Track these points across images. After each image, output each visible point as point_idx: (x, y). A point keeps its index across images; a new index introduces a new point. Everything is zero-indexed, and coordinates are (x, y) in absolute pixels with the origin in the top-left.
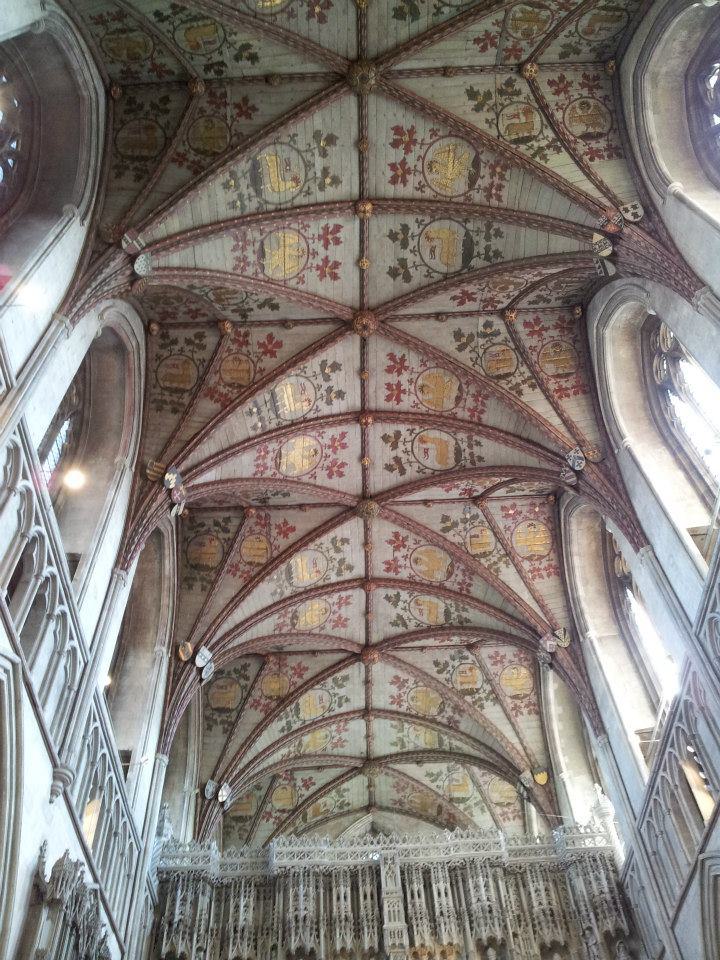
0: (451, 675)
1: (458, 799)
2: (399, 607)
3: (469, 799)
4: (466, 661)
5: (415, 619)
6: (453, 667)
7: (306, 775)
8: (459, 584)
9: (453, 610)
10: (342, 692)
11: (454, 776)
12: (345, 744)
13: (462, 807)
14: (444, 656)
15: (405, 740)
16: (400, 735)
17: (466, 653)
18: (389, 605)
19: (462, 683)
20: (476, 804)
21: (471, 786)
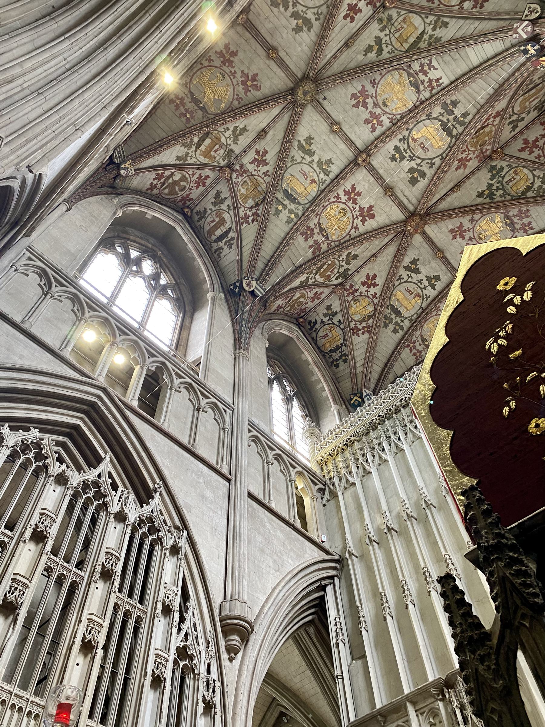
0: (339, 261)
1: (204, 140)
2: (425, 279)
3: (196, 151)
4: (336, 277)
5: (406, 281)
6: (342, 266)
7: (360, 19)
8: (414, 342)
9: (398, 319)
10: (406, 165)
11: (222, 151)
12: (354, 102)
13: (196, 140)
14: (354, 265)
15: (308, 159)
16: (316, 158)
17: (340, 280)
18: (432, 275)
19: (329, 265)
20: (187, 154)
21: (203, 160)
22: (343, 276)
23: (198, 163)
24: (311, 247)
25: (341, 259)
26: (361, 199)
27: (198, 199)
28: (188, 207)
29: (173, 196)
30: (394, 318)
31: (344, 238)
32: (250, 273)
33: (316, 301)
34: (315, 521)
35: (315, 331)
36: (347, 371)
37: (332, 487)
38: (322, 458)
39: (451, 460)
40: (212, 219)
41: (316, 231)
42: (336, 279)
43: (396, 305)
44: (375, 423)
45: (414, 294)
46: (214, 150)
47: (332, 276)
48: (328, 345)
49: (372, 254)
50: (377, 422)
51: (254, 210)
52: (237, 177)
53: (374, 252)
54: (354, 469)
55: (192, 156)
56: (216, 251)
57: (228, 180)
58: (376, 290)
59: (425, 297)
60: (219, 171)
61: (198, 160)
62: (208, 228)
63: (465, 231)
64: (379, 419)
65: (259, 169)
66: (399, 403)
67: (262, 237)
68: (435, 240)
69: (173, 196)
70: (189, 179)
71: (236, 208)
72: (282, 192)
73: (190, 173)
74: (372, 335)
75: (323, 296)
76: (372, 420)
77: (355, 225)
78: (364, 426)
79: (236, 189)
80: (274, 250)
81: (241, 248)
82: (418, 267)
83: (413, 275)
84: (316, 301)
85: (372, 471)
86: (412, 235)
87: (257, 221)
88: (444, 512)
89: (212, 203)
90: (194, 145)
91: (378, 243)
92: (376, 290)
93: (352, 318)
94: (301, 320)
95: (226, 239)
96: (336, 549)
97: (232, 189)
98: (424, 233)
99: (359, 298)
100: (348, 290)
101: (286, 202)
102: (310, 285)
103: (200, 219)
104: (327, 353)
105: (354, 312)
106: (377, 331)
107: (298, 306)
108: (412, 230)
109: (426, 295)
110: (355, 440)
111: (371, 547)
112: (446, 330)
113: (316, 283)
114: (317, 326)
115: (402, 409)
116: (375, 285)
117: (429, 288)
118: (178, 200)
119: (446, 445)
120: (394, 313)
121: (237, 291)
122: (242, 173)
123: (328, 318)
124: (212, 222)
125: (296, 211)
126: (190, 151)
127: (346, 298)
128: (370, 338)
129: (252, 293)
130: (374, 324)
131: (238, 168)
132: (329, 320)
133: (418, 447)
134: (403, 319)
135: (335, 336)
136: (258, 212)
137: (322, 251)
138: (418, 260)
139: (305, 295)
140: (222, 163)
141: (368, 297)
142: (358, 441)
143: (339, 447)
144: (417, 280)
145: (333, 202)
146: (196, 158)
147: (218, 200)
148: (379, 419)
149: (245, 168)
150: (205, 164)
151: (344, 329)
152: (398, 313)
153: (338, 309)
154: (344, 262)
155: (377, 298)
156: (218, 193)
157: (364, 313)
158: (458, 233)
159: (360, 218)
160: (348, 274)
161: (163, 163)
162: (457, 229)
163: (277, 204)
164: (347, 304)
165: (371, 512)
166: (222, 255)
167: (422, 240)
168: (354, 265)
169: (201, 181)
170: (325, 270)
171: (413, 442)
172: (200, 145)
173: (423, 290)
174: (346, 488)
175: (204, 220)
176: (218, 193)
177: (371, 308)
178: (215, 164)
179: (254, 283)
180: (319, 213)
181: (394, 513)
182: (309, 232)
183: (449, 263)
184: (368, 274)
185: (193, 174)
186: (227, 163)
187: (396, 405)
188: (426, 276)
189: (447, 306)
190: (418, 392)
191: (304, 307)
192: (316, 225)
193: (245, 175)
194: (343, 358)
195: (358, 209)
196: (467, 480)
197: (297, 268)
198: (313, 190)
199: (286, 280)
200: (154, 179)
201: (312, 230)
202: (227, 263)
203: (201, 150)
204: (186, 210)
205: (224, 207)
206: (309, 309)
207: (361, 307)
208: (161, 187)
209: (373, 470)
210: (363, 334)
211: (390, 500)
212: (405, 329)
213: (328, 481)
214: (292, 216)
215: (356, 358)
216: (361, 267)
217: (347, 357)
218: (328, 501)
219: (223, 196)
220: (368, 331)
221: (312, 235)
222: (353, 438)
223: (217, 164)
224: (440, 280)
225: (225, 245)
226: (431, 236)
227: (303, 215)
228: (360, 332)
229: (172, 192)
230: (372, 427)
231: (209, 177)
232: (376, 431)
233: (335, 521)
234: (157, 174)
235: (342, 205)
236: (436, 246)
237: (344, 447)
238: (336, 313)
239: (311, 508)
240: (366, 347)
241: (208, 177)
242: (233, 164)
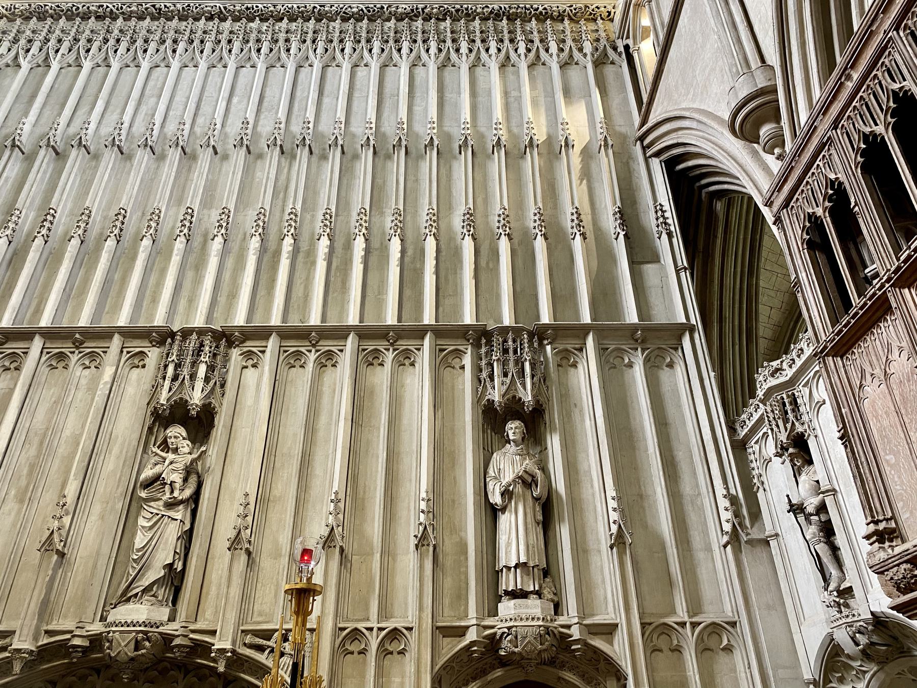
44: (47, 12)
50: (50, 11)
64: (55, 10)
66: (94, 8)
76: (45, 5)
78: (30, 5)
110: (6, 16)
115: (93, 18)
171: (70, 66)
230: (39, 13)
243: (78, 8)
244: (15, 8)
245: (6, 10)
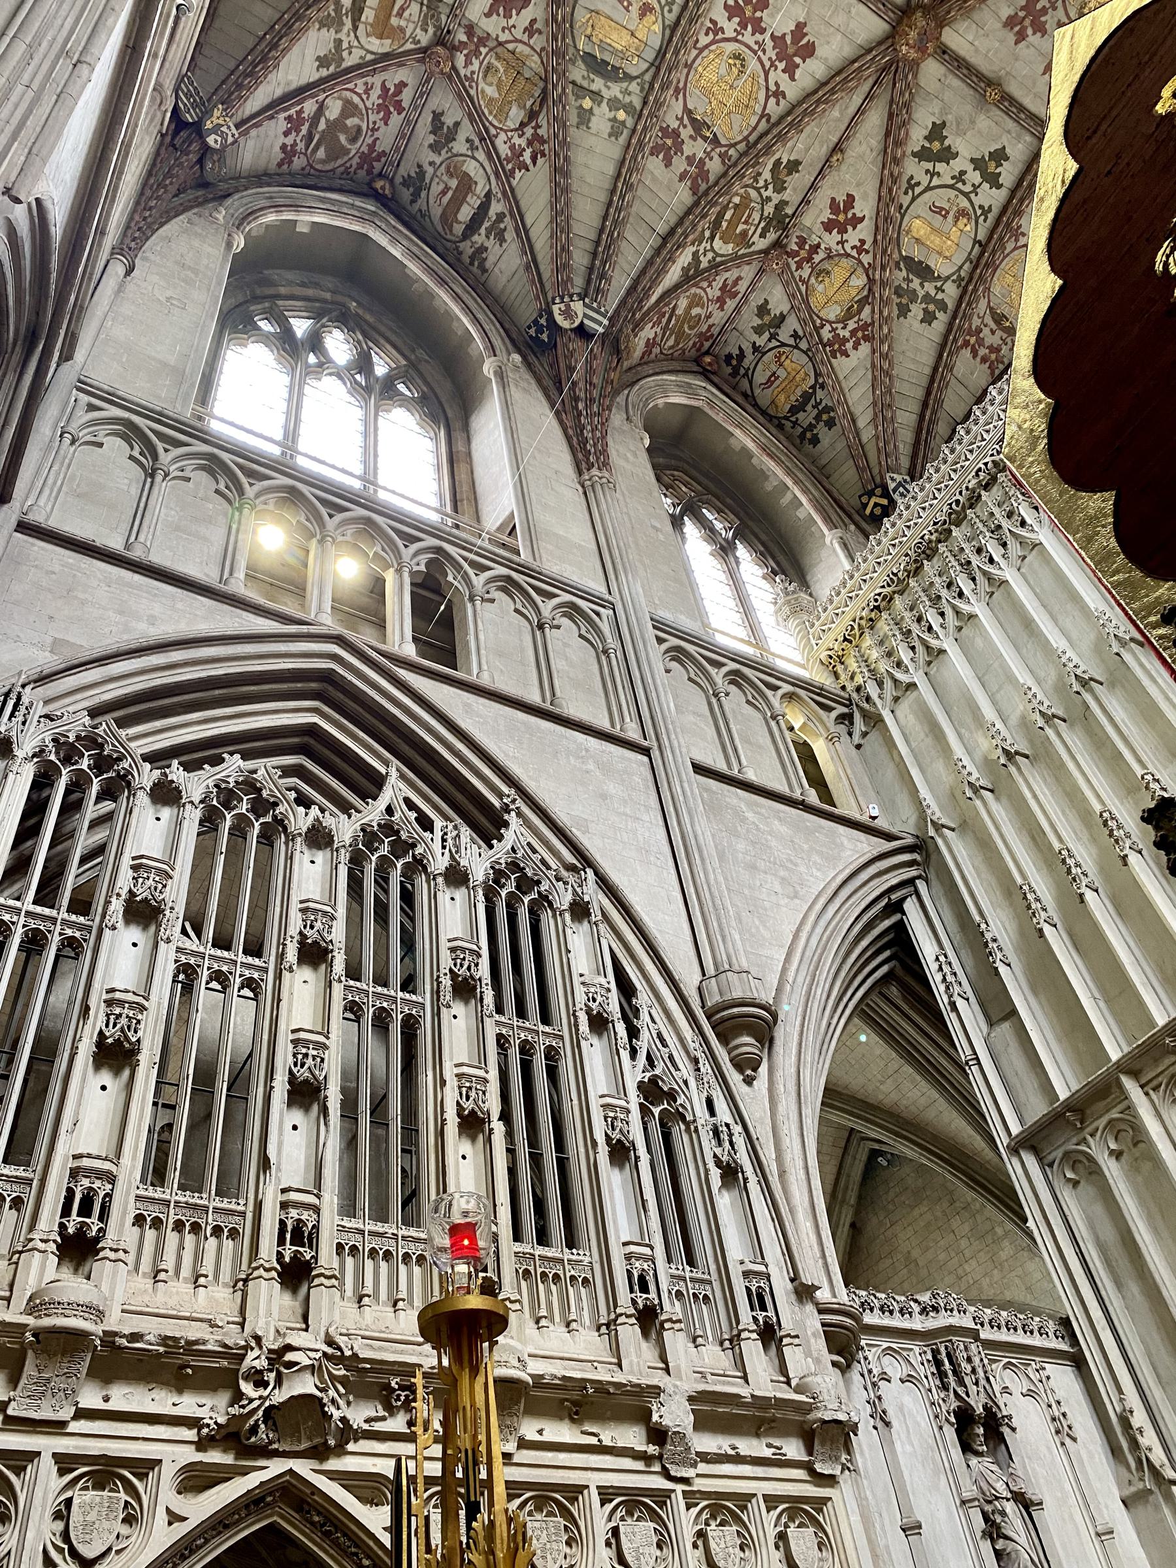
0: (757, 189)
2: (969, 167)
3: (355, 28)
4: (759, 230)
5: (928, 188)
6: (769, 199)
9: (930, 287)
17: (772, 236)
19: (736, 206)
20: (338, 42)
21: (378, 46)
22: (774, 223)
23: (369, 57)
24: (682, 177)
25: (761, 183)
26: (772, 16)
27: (398, 148)
28: (380, 175)
29: (340, 162)
30: (918, 288)
31: (755, 128)
32: (563, 286)
33: (730, 304)
34: (846, 783)
35: (746, 374)
36: (841, 445)
37: (866, 706)
38: (830, 653)
39: (1122, 556)
40: (441, 186)
41: (686, 133)
42: (762, 235)
43: (917, 254)
44: (930, 541)
45: (951, 214)
46: (395, 12)
47: (751, 233)
48: (782, 397)
49: (831, 146)
50: (933, 538)
51: (529, 131)
52: (468, 63)
53: (835, 140)
54: (905, 655)
55: (350, 47)
56: (472, 258)
57: (450, 77)
58: (863, 232)
59: (979, 212)
60: (421, 61)
61: (368, 52)
62: (439, 211)
63: (1044, 11)
64: (936, 531)
65: (511, 22)
66: (974, 482)
67: (566, 190)
68: (973, 59)
69: (340, 162)
70: (361, 106)
71: (486, 139)
72: (580, 63)
73: (360, 90)
74: (877, 343)
75: (742, 287)
76: (922, 538)
77: (773, 88)
78: (907, 555)
79: (473, 92)
80: (599, 210)
81: (527, 232)
82: (947, 143)
83: (940, 167)
84: (730, 304)
85: (945, 646)
86: (914, 65)
87: (543, 155)
88: (1123, 687)
89: (430, 146)
90: (347, 14)
91: (837, 115)
92: (863, 232)
93: (821, 319)
94: (708, 359)
95: (486, 224)
96: (904, 824)
97: (464, 96)
98: (944, 52)
99: (826, 265)
100: (797, 254)
101: (598, 84)
102: (706, 270)
103: (416, 196)
104: (786, 418)
105: (822, 300)
106: (886, 330)
107: (691, 328)
108: (913, 54)
109: (981, 207)
110: (894, 592)
111: (978, 803)
112: (1050, 260)
113: (718, 259)
114: (746, 363)
115: (983, 493)
116: (856, 221)
117: (986, 186)
118: (354, 166)
119: (1103, 526)
120: (918, 276)
121: (545, 337)
122: (477, 47)
123: (767, 335)
124: (444, 193)
125: (627, 99)
126: (342, 36)
127: (796, 274)
128: (874, 352)
129: (582, 332)
130: (877, 316)
131: (464, 38)
132: (769, 340)
133: (1036, 565)
134: (939, 284)
135: (793, 373)
136: (540, 132)
137: (712, 178)
138: (944, 124)
139: (701, 298)
140: (425, 39)
141: (848, 255)
142: (901, 592)
143: (861, 618)
144: (953, 178)
145: (707, 46)
146: (362, 47)
147: (443, 136)
148: (936, 531)
149: (479, 33)
150: (386, 56)
151: (809, 349)
152: (924, 271)
153: (785, 307)
154: (771, 187)
155: (867, 252)
156: (437, 116)
157: (847, 297)
158: (1027, 22)
159: (781, 66)
160: (787, 215)
161: (294, 86)
162: (1022, 14)
163: (578, 97)
164: (803, 288)
165: (963, 731)
166: (488, 265)
167: (942, 70)
168: (794, 190)
169: (390, 101)
170: (729, 222)
171: (1025, 557)
172: (361, 11)
173: (972, 196)
174: (896, 699)
175: (423, 194)
176: (437, 116)
177: (859, 281)
178: (409, 46)
179: (578, 307)
180: (681, 85)
181: (1014, 720)
182: (669, 142)
183: (1022, 108)
184: (833, 199)
185: (367, 91)
186: (435, 34)
187: (967, 488)
188: (972, 160)
189: (1042, 200)
190: (1014, 428)
191: (704, 328)
192: (681, 119)
193: (484, 50)
194: (825, 417)
195: (769, 44)
196: (1169, 589)
197: (665, 239)
198: (652, 31)
199: (648, 276)
200: (286, 134)
201: (676, 134)
202: (503, 280)
203: (365, 23)
204: (379, 184)
205: (459, 146)
206: (718, 329)
207: (837, 286)
208: (307, 148)
209: (948, 644)
210: (855, 348)
211: (998, 696)
212: (951, 305)
213: (855, 695)
214: (621, 115)
215: (852, 409)
216: (813, 187)
217: (832, 414)
218: (864, 735)
219: (449, 121)
220: (866, 338)
221: (679, 146)
222: (889, 589)
223: (413, 46)
224: (1007, 159)
225: (488, 237)
226: (962, 53)
227: (645, 103)
228: (849, 345)
229: (336, 151)
230: (924, 552)
231: (406, 85)
232: (935, 559)
233: (890, 772)
234: (289, 119)
235: (730, 47)
236: (980, 76)
237: (873, 615)
238: (782, 318)
239: (832, 758)
240: (870, 377)
241: (402, 85)
242: (449, 32)
243: (958, 502)
244: (895, 575)
245: (889, 586)
